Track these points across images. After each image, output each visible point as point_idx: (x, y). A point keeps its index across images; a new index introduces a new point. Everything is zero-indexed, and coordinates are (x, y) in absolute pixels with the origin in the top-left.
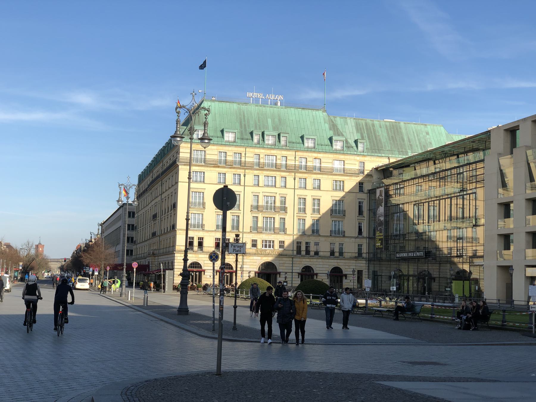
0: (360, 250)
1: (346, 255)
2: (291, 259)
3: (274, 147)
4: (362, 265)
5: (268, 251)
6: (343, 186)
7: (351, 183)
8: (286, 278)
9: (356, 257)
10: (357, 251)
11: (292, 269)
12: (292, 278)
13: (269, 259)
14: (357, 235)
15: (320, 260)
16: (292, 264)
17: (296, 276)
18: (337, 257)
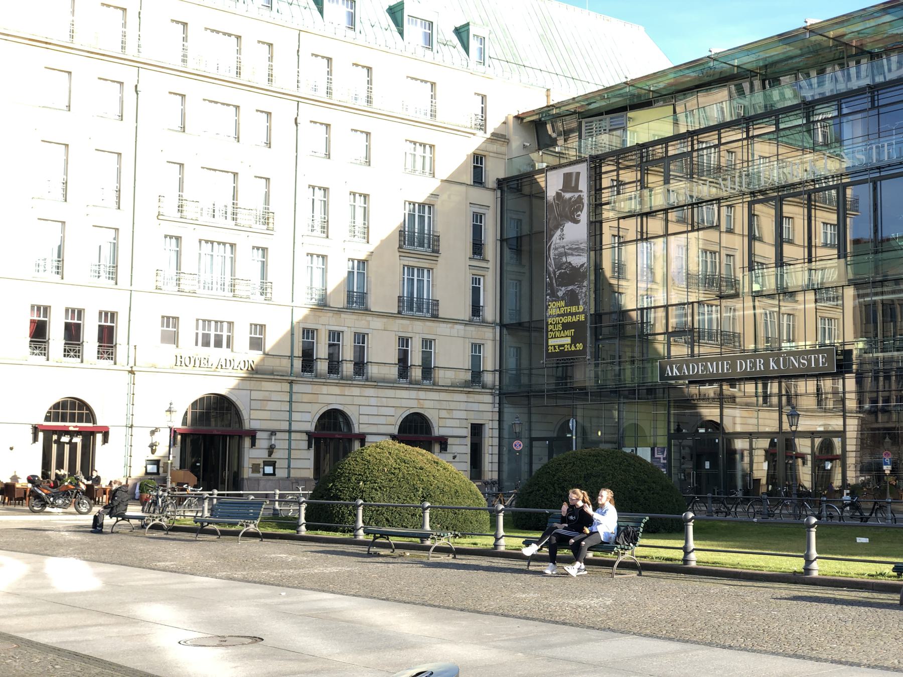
0: (476, 360)
1: (443, 377)
2: (286, 387)
4: (482, 407)
6: (432, 160)
7: (454, 155)
8: (271, 449)
9: (466, 384)
10: (468, 364)
11: (290, 421)
12: (290, 449)
13: (223, 386)
14: (465, 312)
16: (290, 402)
17: (300, 441)
18: (417, 383)
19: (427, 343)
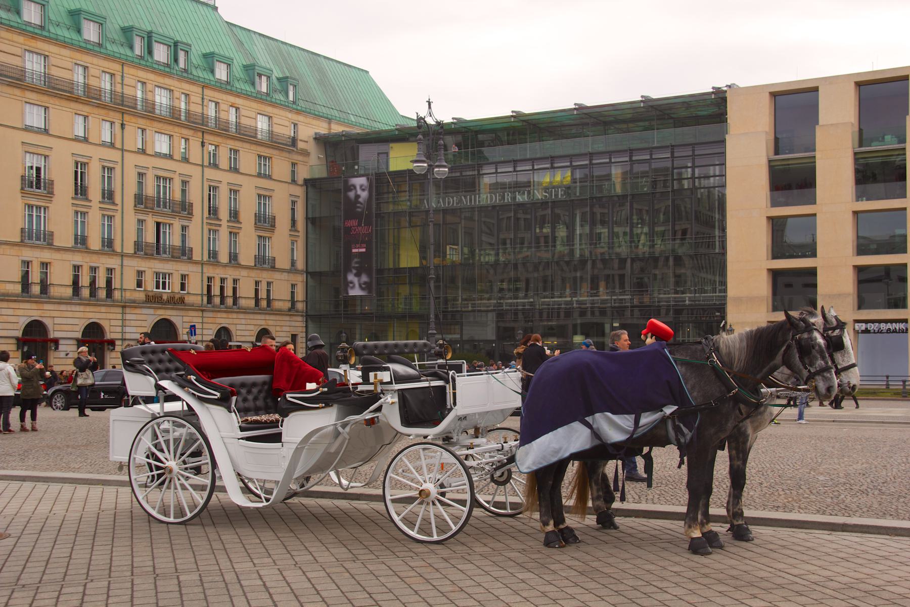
3: (166, 70)
14: (287, 266)
15: (242, 316)
19: (269, 284)
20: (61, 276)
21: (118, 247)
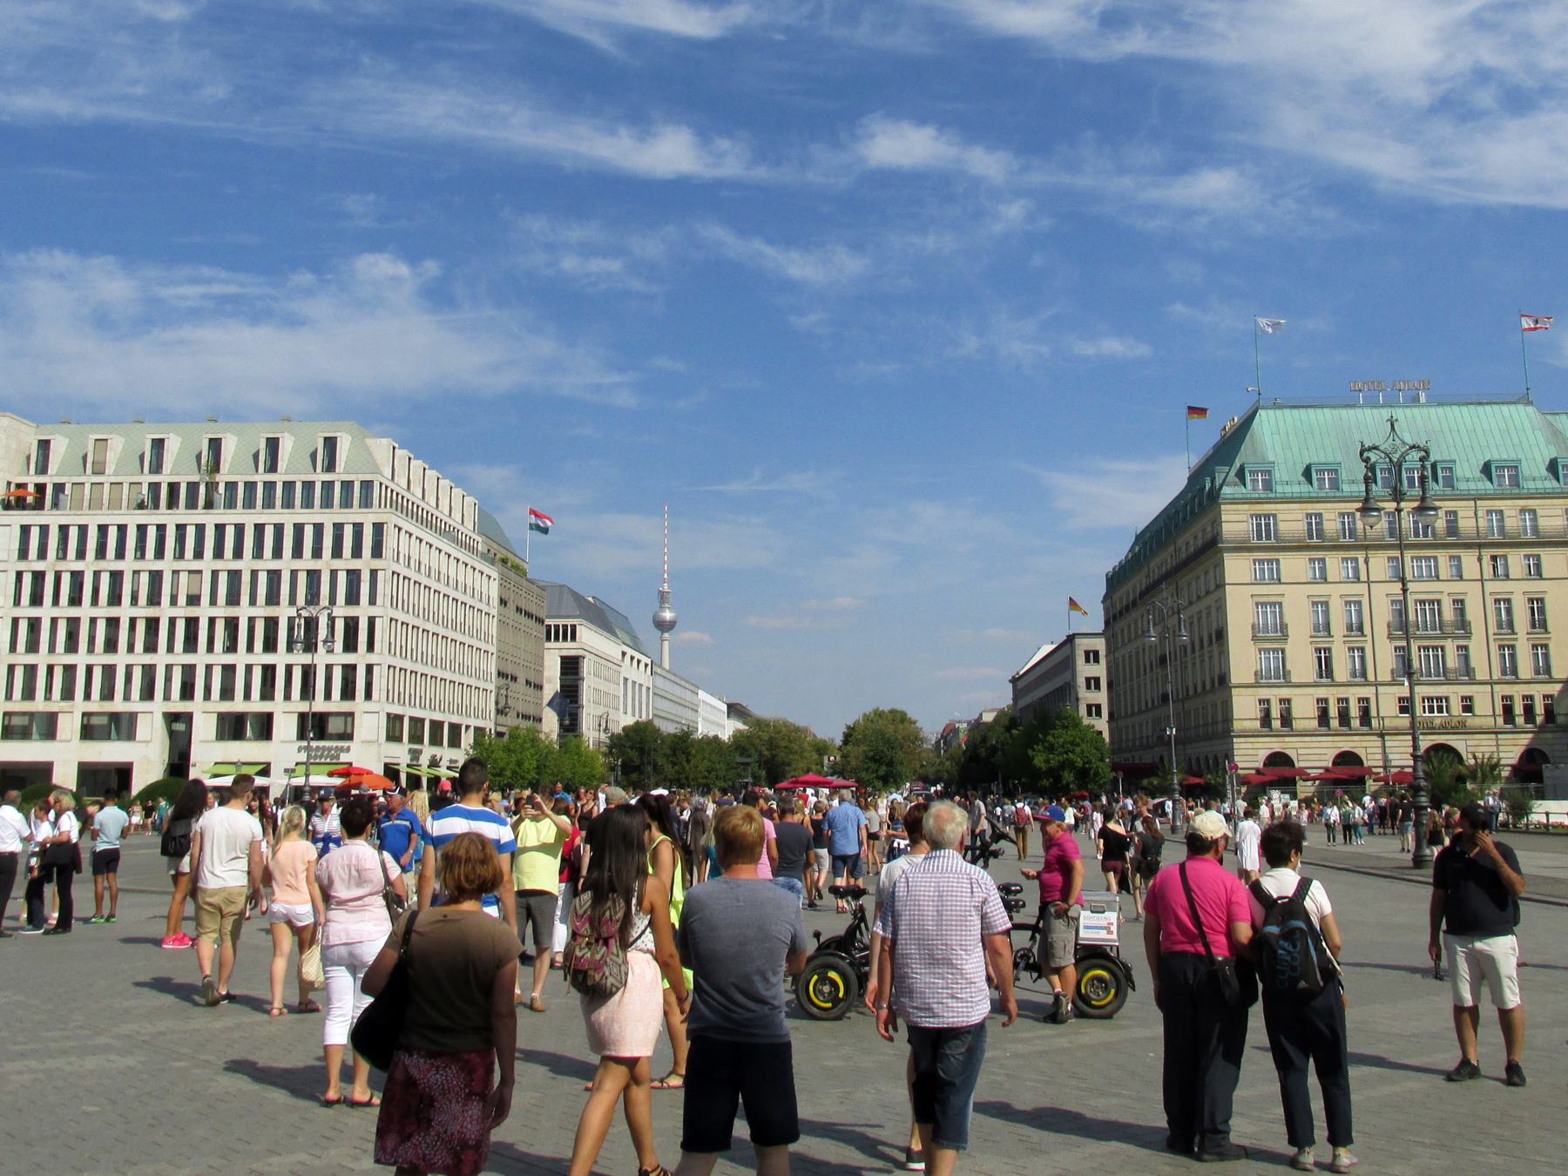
5: (1437, 722)
20: (1304, 710)
21: (1371, 677)
